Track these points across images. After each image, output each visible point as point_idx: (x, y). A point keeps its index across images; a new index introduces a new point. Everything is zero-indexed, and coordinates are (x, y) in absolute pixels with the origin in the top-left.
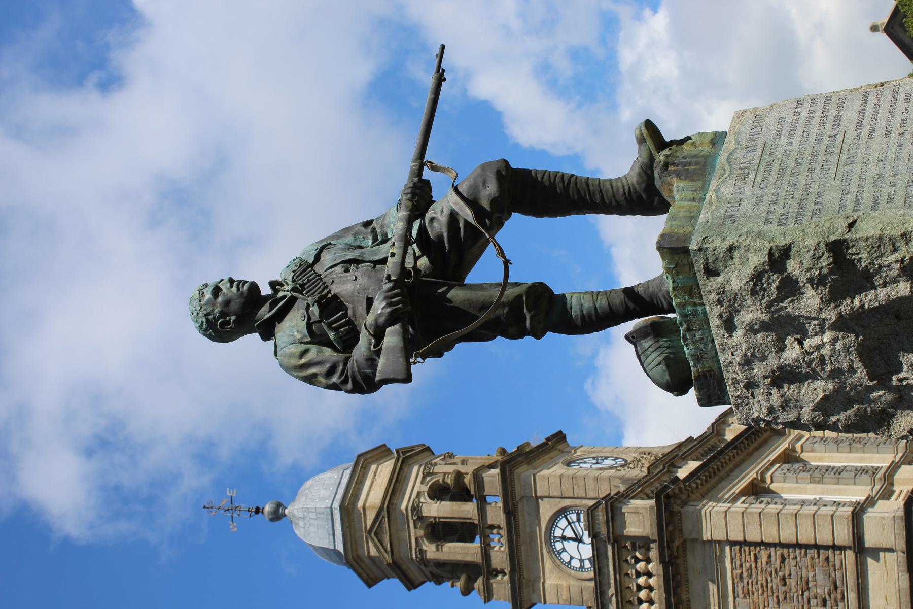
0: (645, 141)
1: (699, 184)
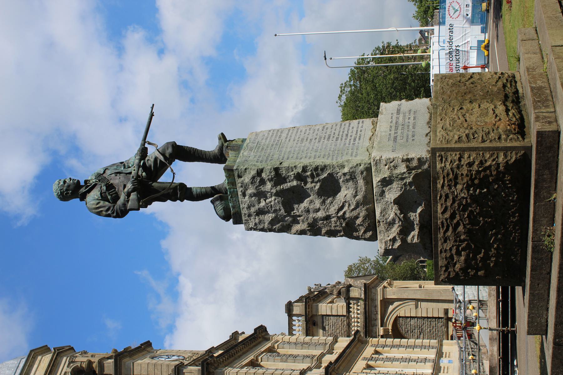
0: (221, 139)
1: (237, 152)
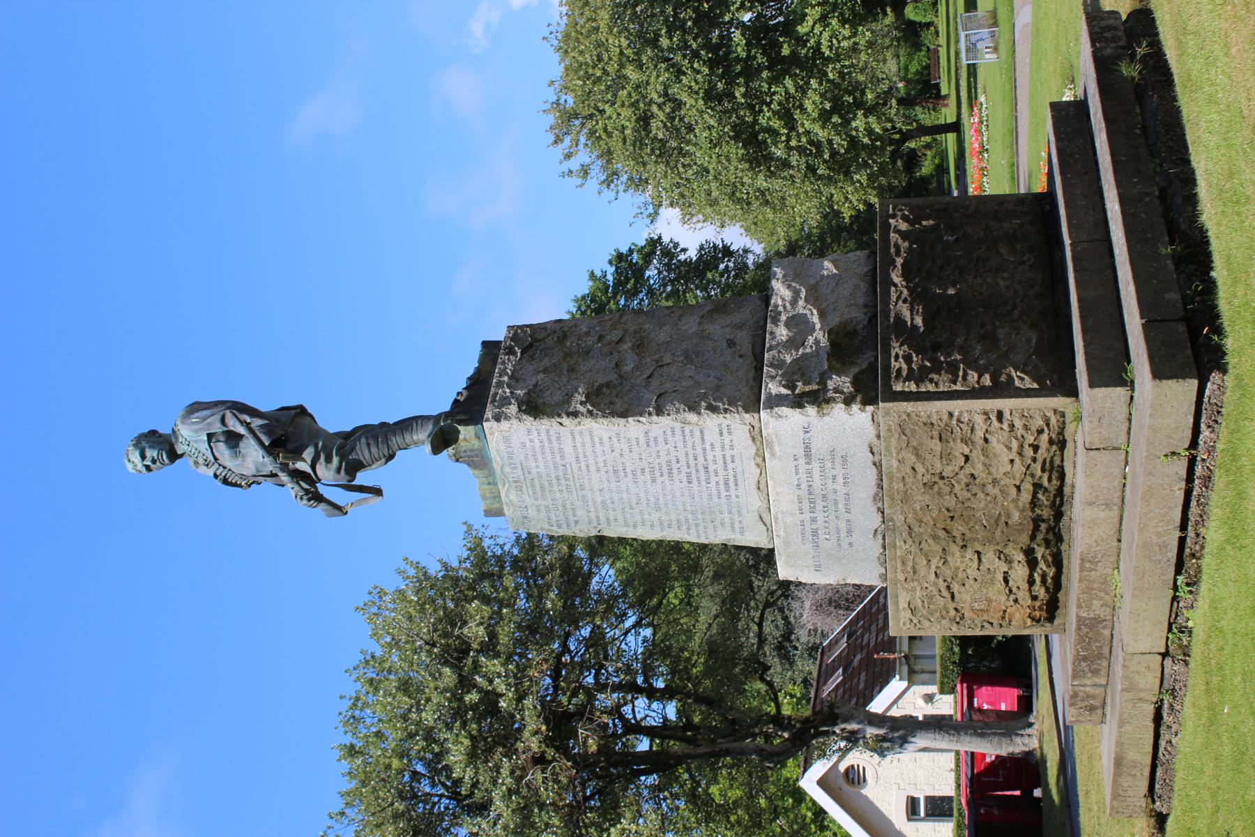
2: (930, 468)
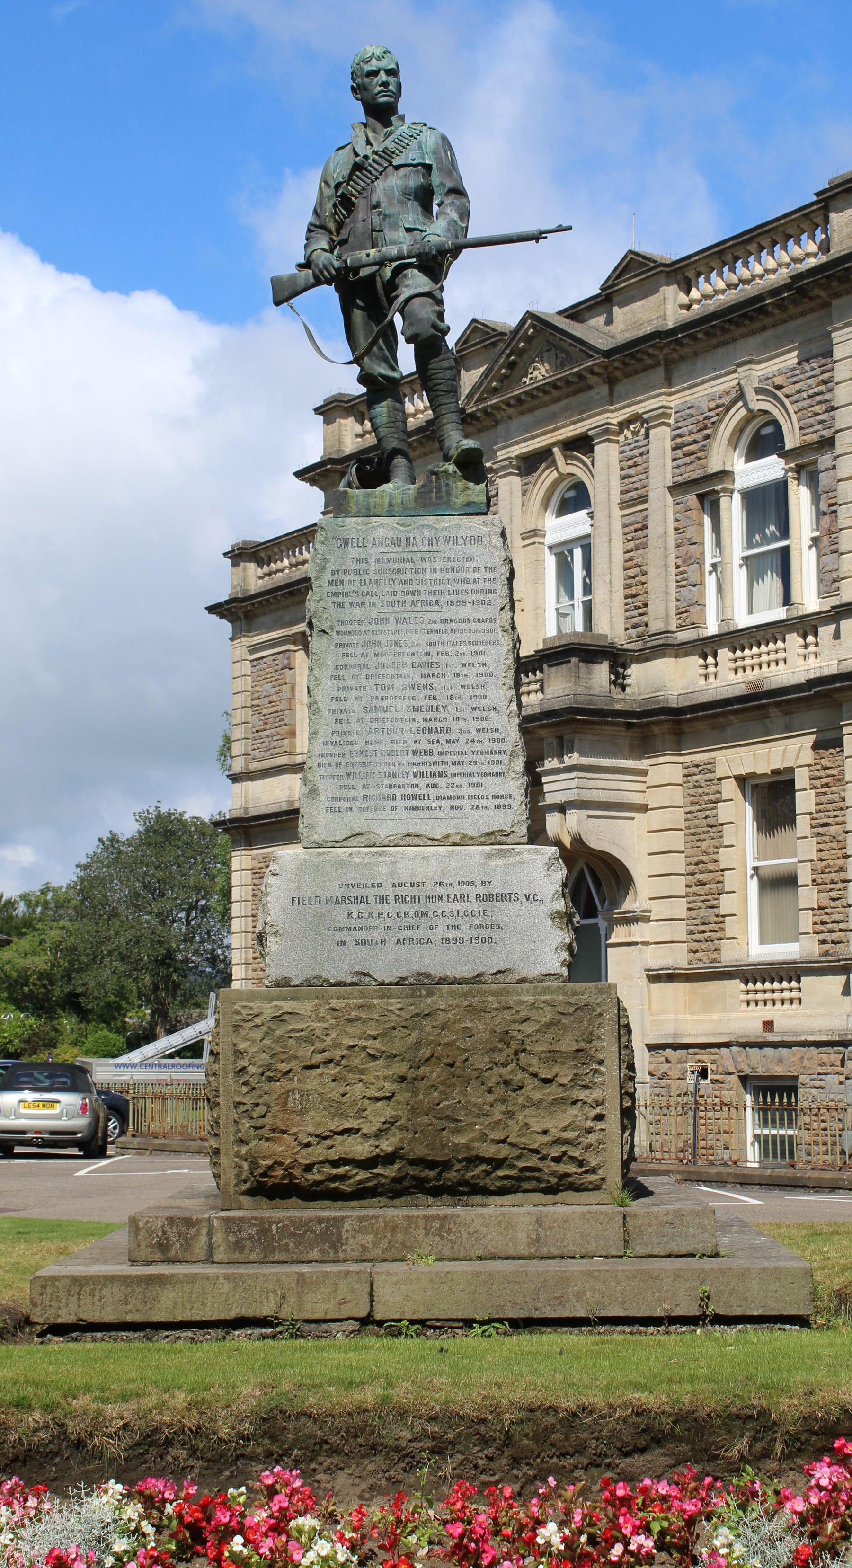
1: (412, 505)
2: (534, 1039)
